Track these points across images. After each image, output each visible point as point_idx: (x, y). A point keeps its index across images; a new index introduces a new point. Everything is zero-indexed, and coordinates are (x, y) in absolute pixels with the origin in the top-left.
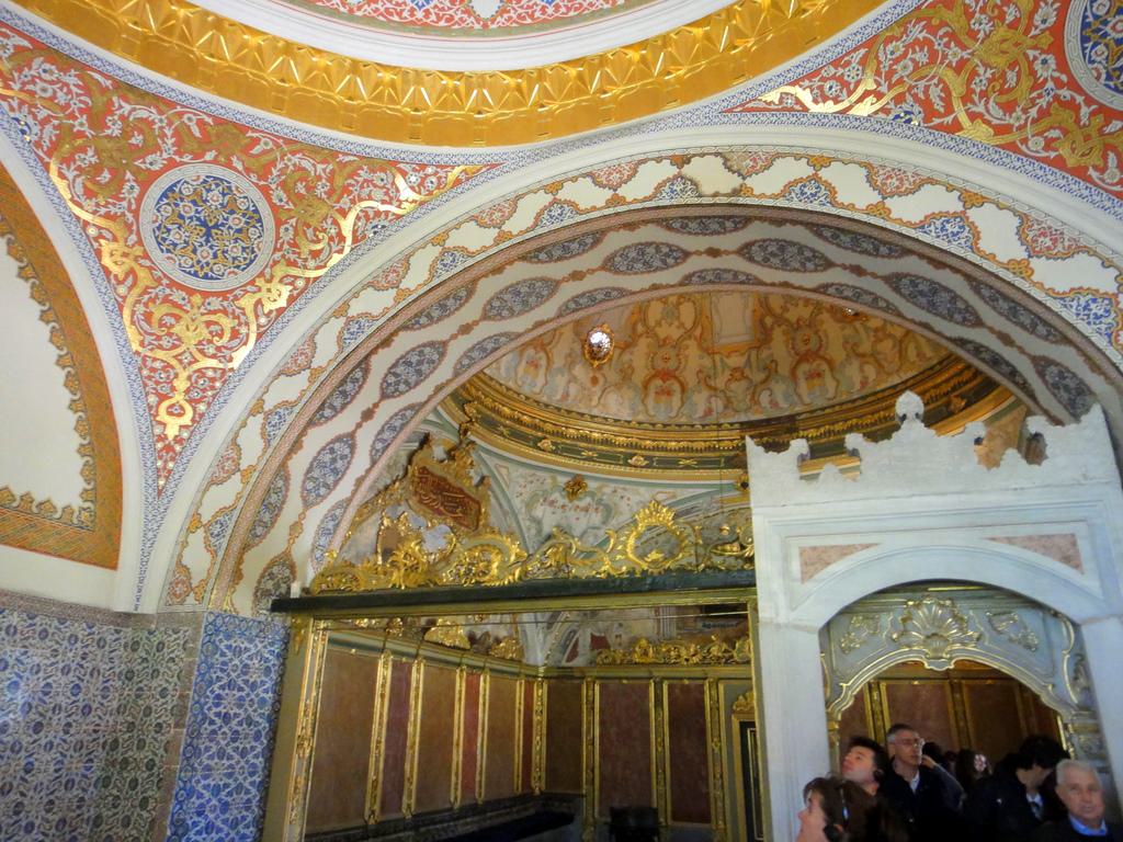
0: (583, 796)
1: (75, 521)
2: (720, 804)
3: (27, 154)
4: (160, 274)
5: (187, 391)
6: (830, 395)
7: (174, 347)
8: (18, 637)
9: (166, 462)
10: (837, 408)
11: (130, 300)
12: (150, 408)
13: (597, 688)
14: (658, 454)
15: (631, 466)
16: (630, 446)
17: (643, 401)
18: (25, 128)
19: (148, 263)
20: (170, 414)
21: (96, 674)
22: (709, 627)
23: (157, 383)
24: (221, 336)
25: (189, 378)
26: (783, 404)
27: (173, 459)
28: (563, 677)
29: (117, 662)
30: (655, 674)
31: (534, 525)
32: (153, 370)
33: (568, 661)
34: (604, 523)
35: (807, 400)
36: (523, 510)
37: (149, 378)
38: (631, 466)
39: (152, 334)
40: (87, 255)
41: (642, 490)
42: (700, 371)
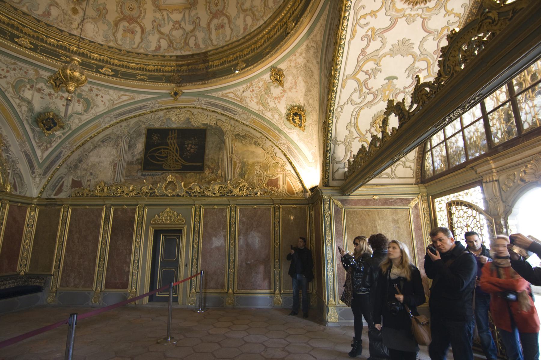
0: (51, 275)
2: (135, 278)
6: (228, 38)
10: (230, 46)
13: (70, 211)
14: (122, 69)
15: (101, 73)
16: (103, 61)
17: (114, 34)
22: (144, 175)
26: (202, 46)
28: (50, 205)
30: (106, 202)
33: (56, 195)
34: (86, 111)
35: (215, 43)
36: (11, 90)
38: (101, 73)
41: (111, 92)
42: (154, 21)
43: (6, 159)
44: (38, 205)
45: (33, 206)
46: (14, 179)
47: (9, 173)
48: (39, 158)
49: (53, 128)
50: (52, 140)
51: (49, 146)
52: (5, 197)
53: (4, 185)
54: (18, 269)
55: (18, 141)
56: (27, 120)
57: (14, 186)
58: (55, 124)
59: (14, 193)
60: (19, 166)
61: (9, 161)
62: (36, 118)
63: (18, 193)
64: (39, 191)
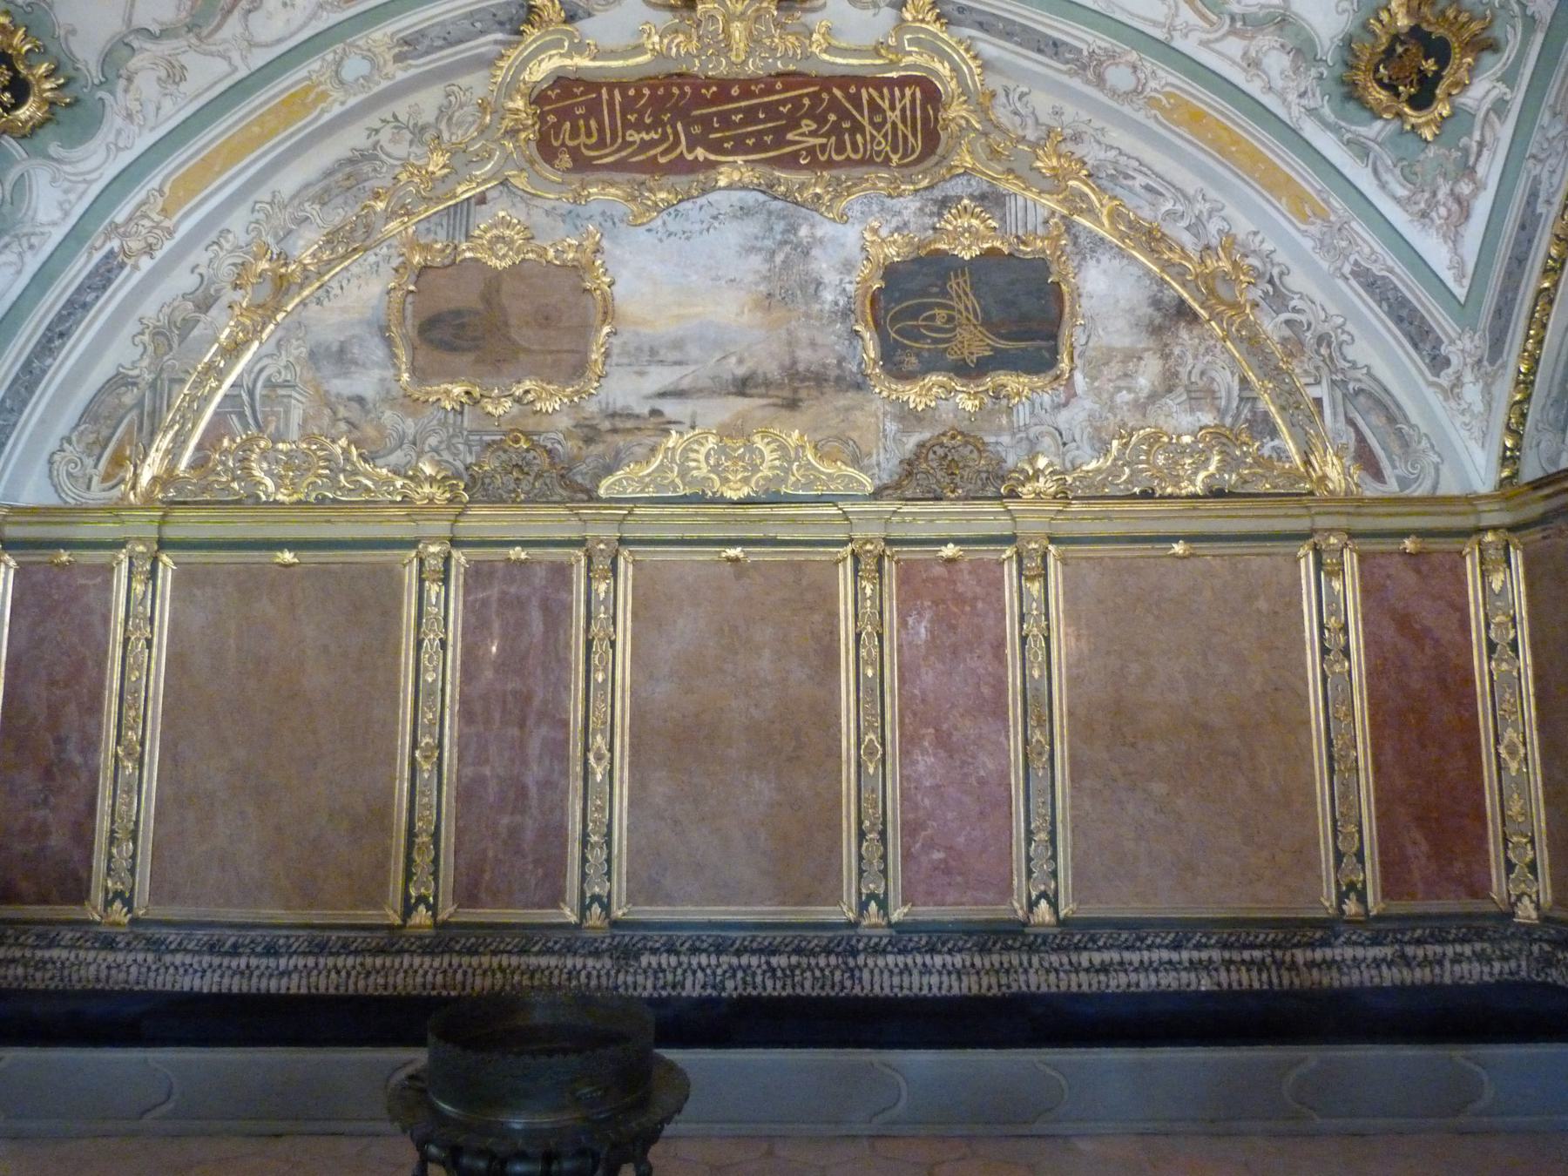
31: (1266, 41)
36: (1187, 14)
43: (1284, 341)
44: (1513, 528)
45: (1489, 537)
46: (1351, 422)
47: (1318, 402)
48: (1448, 277)
49: (1438, 77)
50: (1466, 151)
51: (1465, 188)
52: (1322, 522)
53: (1307, 463)
54: (1499, 887)
55: (1304, 233)
56: (1312, 112)
57: (1366, 460)
58: (1441, 52)
59: (1371, 490)
60: (1361, 352)
61: (1302, 344)
62: (1343, 83)
63: (1392, 487)
64: (1496, 452)
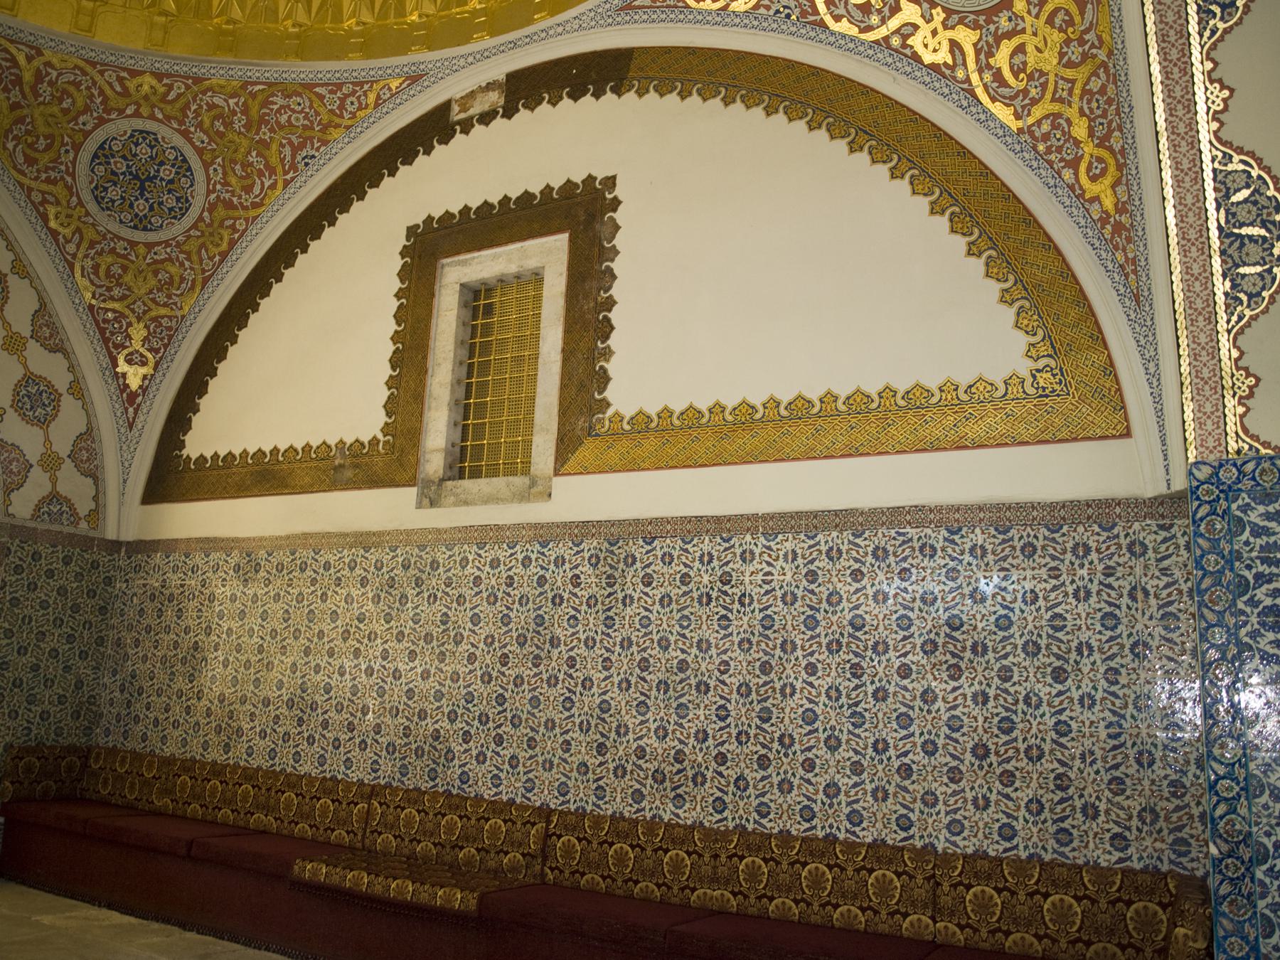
1: (1031, 391)
3: (804, 31)
4: (972, 17)
5: (1091, 134)
7: (1044, 86)
8: (990, 558)
9: (1124, 250)
11: (975, 78)
12: (1071, 188)
18: (787, 11)
19: (956, 17)
20: (1094, 179)
21: (1140, 596)
23: (1059, 150)
24: (1070, 22)
25: (1082, 113)
27: (1129, 240)
29: (1177, 574)
32: (1046, 137)
37: (1049, 151)
39: (1017, 95)
40: (909, 69)
